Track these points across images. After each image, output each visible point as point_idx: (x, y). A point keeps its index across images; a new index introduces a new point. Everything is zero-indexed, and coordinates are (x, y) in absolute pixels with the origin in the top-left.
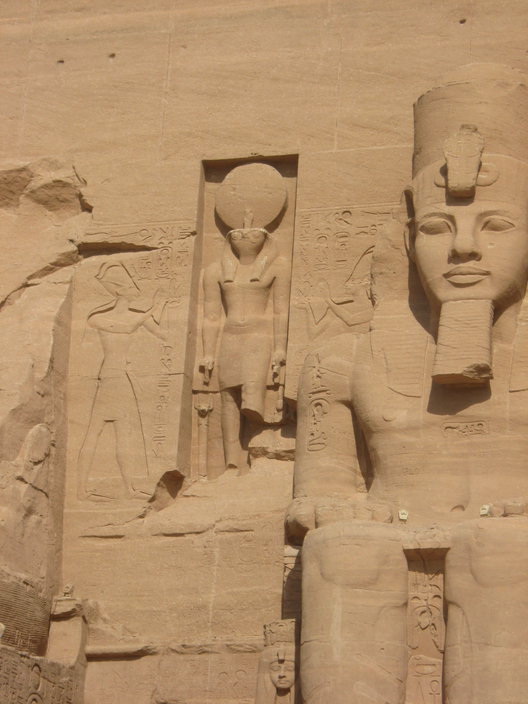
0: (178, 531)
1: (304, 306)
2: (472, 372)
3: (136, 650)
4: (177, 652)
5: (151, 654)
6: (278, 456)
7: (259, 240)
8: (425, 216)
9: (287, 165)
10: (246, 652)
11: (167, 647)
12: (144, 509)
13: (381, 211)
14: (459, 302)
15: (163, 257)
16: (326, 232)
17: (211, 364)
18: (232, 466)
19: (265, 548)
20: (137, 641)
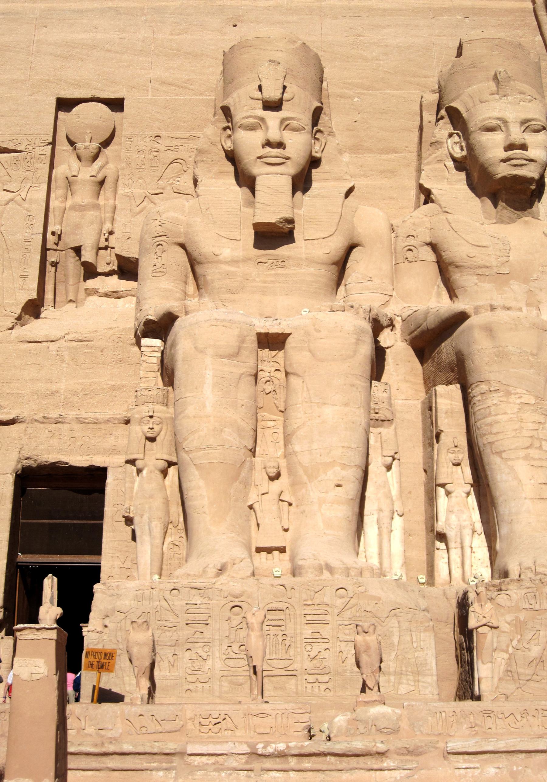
0: (37, 340)
1: (129, 194)
2: (282, 222)
3: (8, 419)
4: (39, 422)
5: (20, 422)
6: (106, 295)
7: (95, 151)
8: (243, 118)
9: (116, 105)
10: (90, 423)
11: (31, 418)
12: (13, 324)
13: (182, 137)
14: (270, 175)
15: (28, 157)
16: (143, 148)
17: (59, 231)
18: (71, 301)
19: (102, 353)
20: (9, 413)
